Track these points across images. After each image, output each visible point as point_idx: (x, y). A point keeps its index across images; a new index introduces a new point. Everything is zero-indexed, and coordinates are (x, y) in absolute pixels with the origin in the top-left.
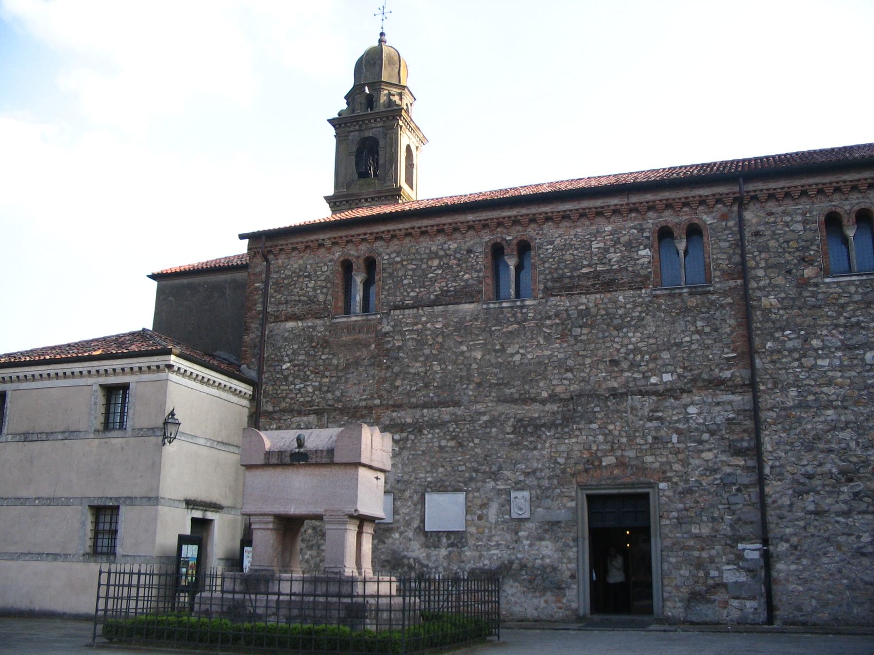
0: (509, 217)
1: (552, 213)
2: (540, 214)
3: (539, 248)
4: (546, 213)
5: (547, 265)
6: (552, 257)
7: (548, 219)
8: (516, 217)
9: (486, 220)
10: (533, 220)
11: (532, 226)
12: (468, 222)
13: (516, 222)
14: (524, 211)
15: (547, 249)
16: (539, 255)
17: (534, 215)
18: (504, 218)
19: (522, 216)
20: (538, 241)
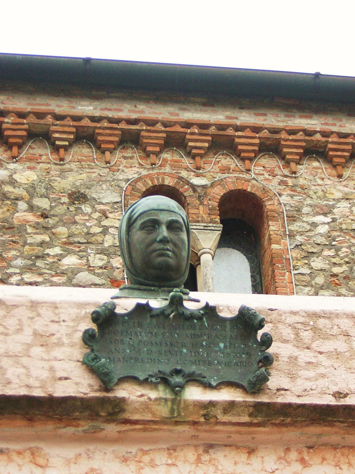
0: (204, 126)
1: (325, 134)
2: (292, 132)
3: (292, 219)
4: (309, 133)
5: (317, 263)
6: (330, 246)
7: (315, 151)
8: (222, 127)
9: (135, 122)
10: (271, 147)
11: (268, 162)
12: (77, 118)
13: (223, 143)
14: (246, 118)
15: (314, 225)
16: (292, 236)
17: (275, 131)
18: (188, 125)
19: (238, 128)
20: (284, 199)
